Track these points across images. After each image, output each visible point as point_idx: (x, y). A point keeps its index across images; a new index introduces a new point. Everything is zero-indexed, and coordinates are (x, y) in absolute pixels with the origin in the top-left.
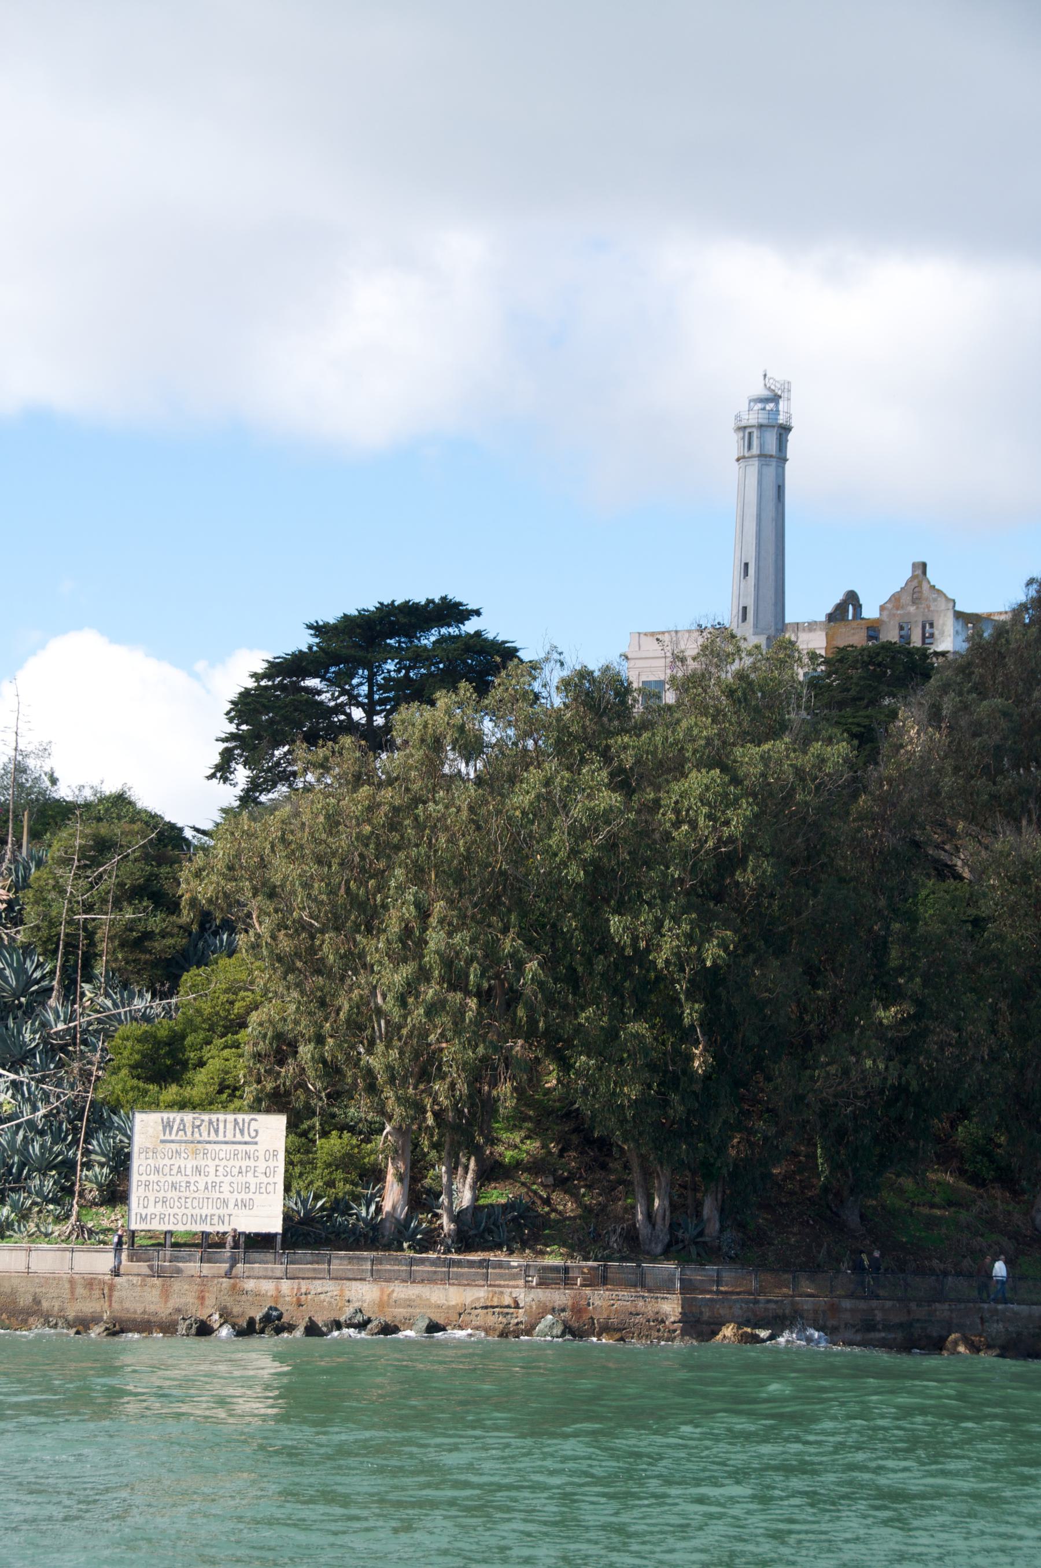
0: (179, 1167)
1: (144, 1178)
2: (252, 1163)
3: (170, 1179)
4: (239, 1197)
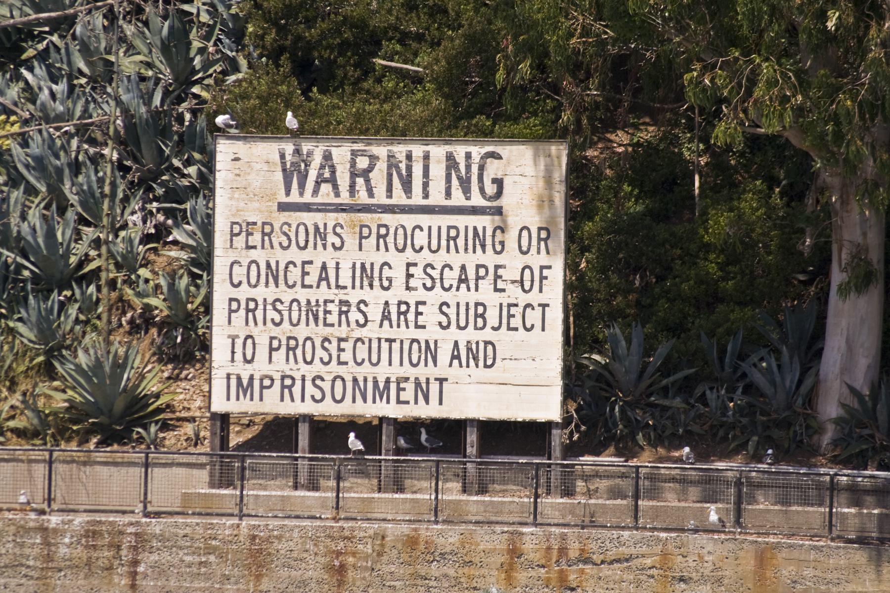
0: (324, 267)
1: (244, 292)
2: (490, 259)
3: (302, 295)
4: (463, 337)
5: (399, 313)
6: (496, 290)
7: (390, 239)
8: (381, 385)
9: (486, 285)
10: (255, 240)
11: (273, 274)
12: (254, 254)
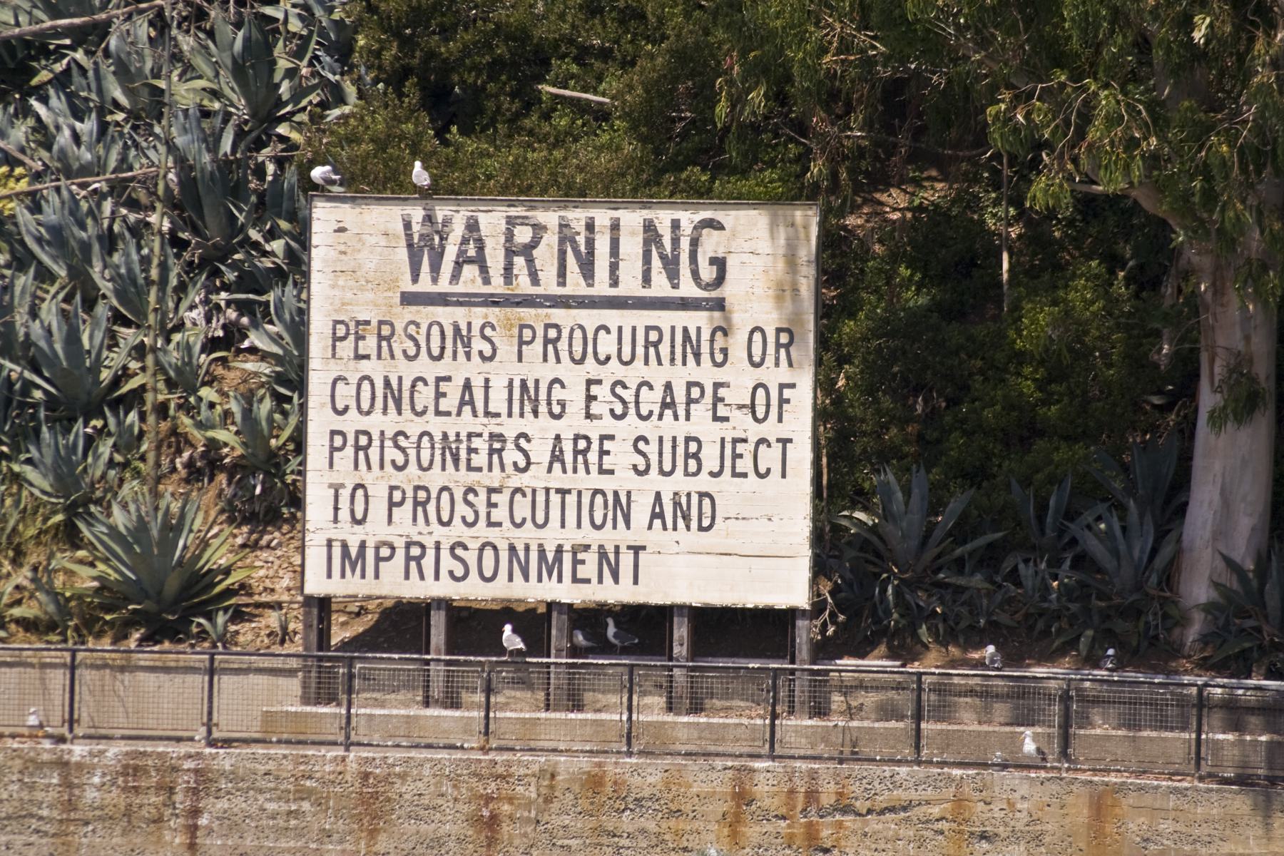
0: (467, 386)
1: (352, 422)
2: (706, 374)
3: (436, 426)
4: (667, 487)
5: (576, 452)
6: (716, 418)
7: (563, 345)
8: (550, 556)
9: (701, 411)
10: (368, 346)
11: (394, 396)
12: (366, 367)
